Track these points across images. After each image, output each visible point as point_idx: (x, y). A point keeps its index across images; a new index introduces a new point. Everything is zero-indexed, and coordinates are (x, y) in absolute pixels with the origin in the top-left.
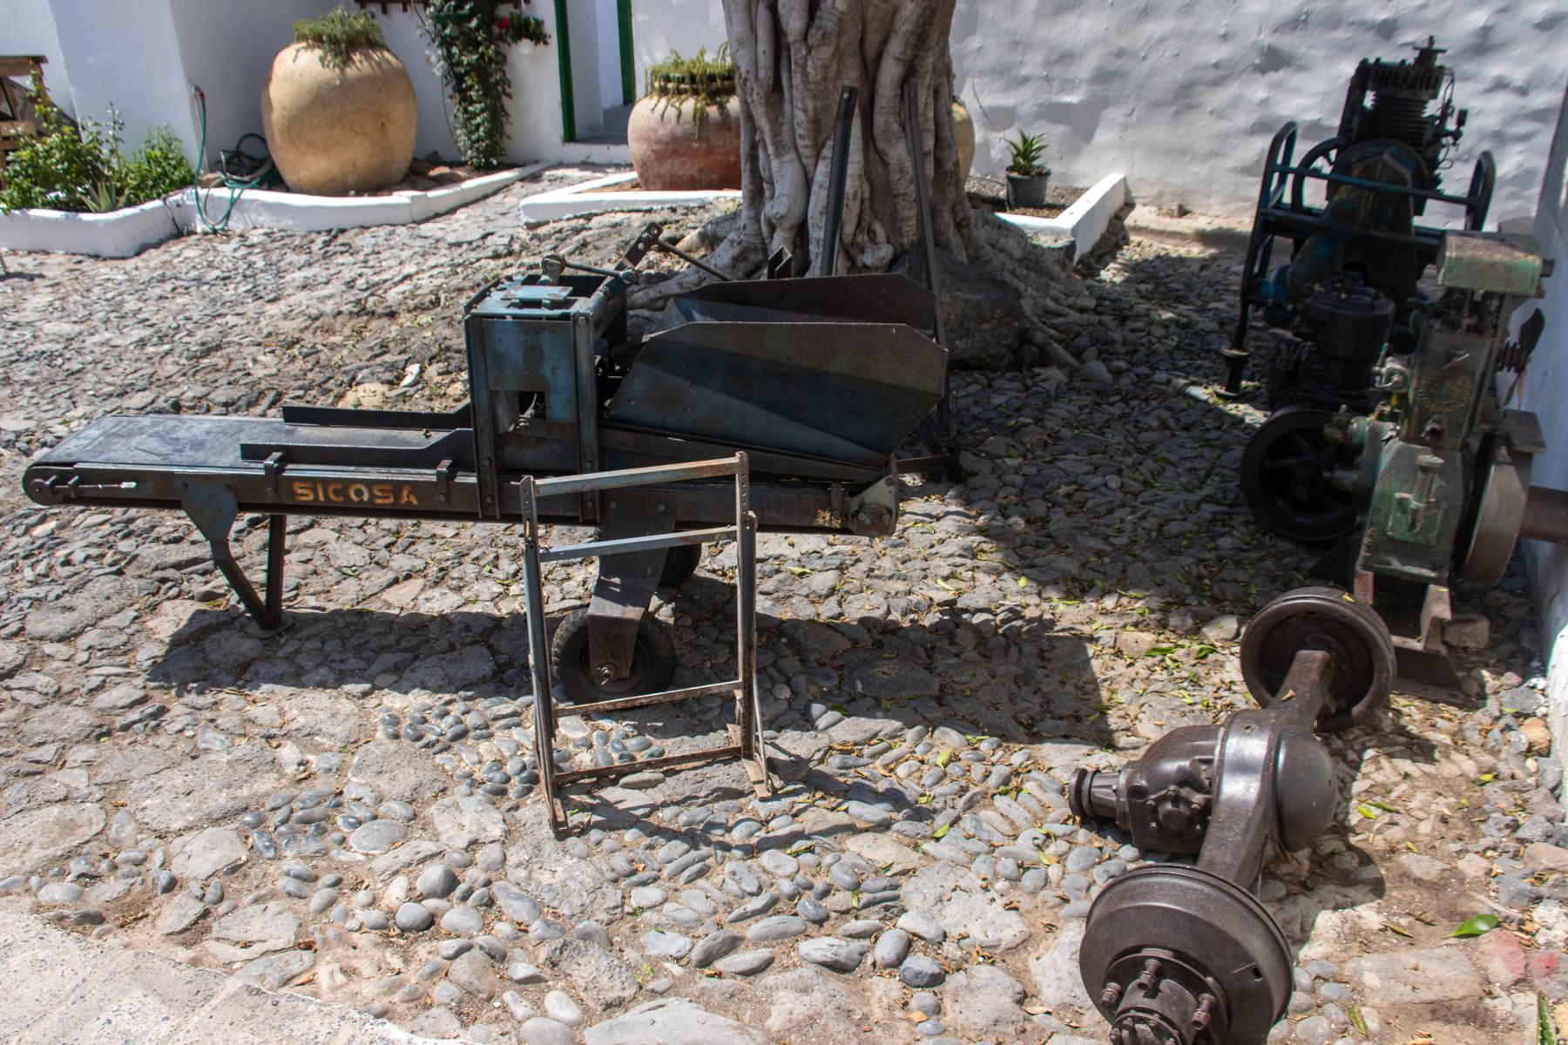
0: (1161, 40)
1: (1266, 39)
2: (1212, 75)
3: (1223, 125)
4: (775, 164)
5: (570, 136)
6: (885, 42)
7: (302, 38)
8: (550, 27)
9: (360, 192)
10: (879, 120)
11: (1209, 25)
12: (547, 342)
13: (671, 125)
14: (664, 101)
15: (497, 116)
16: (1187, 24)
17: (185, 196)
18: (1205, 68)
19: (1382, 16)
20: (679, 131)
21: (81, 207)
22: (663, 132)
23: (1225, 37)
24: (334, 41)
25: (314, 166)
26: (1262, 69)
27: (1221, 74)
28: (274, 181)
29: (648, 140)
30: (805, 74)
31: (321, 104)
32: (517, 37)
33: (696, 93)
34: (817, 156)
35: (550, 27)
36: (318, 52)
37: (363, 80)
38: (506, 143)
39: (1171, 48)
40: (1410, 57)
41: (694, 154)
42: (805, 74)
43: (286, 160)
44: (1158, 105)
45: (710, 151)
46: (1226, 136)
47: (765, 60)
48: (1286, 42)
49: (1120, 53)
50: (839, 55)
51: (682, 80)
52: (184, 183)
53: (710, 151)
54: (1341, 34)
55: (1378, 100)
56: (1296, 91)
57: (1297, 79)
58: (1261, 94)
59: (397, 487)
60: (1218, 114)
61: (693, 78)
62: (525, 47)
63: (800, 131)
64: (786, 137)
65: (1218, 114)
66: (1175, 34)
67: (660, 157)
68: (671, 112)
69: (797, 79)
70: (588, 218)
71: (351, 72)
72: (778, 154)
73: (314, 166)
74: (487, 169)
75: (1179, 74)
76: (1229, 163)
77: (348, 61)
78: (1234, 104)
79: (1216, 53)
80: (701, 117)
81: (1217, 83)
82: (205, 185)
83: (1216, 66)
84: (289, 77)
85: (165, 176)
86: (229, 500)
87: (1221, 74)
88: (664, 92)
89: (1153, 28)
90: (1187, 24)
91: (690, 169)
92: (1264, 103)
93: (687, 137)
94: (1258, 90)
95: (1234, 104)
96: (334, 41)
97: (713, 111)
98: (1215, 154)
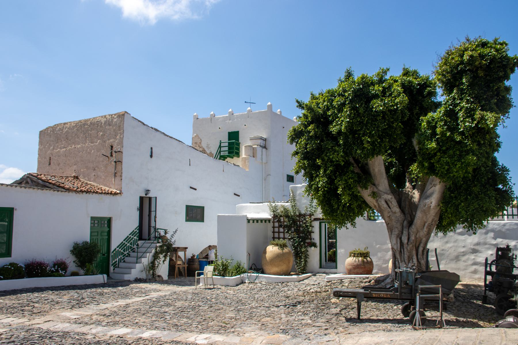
0: (451, 247)
1: (472, 247)
2: (463, 254)
4: (400, 264)
5: (321, 267)
6: (419, 244)
7: (273, 244)
8: (318, 244)
9: (285, 275)
10: (419, 257)
11: (460, 245)
12: (409, 275)
13: (357, 262)
14: (355, 258)
15: (306, 261)
17: (244, 275)
18: (461, 252)
19: (495, 243)
20: (359, 264)
21: (224, 276)
22: (355, 264)
23: (464, 247)
24: (281, 245)
25: (275, 269)
26: (473, 253)
27: (464, 254)
28: (263, 273)
31: (278, 257)
32: (311, 247)
33: (361, 256)
34: (409, 262)
35: (318, 244)
36: (277, 247)
37: (286, 253)
38: (307, 268)
39: (453, 249)
40: (505, 247)
41: (362, 268)
43: (266, 268)
44: (452, 260)
45: (365, 268)
46: (467, 266)
47: (399, 247)
48: (476, 247)
49: (443, 250)
50: (413, 246)
51: (358, 254)
52: (244, 272)
53: (365, 268)
54: (487, 246)
55: (502, 253)
56: (480, 257)
57: (480, 254)
59: (387, 294)
60: (465, 261)
61: (361, 254)
62: (313, 248)
63: (406, 258)
64: (403, 259)
65: (465, 261)
66: (453, 246)
67: (354, 268)
68: (357, 260)
69: (405, 250)
70: (341, 280)
71: (284, 251)
72: (401, 262)
73: (275, 269)
74: (303, 273)
75: (455, 254)
76: (468, 271)
77: (283, 249)
78: (468, 259)
79: (463, 250)
80: (363, 261)
81: (464, 255)
82: (248, 273)
83: (463, 252)
84: (271, 252)
85: (239, 270)
86: (363, 296)
87: (464, 254)
88: (354, 256)
90: (456, 244)
91: (361, 271)
92: (474, 259)
93: (360, 265)
94: (472, 257)
95: (468, 259)
96: (281, 245)
97: (365, 260)
98: (465, 269)
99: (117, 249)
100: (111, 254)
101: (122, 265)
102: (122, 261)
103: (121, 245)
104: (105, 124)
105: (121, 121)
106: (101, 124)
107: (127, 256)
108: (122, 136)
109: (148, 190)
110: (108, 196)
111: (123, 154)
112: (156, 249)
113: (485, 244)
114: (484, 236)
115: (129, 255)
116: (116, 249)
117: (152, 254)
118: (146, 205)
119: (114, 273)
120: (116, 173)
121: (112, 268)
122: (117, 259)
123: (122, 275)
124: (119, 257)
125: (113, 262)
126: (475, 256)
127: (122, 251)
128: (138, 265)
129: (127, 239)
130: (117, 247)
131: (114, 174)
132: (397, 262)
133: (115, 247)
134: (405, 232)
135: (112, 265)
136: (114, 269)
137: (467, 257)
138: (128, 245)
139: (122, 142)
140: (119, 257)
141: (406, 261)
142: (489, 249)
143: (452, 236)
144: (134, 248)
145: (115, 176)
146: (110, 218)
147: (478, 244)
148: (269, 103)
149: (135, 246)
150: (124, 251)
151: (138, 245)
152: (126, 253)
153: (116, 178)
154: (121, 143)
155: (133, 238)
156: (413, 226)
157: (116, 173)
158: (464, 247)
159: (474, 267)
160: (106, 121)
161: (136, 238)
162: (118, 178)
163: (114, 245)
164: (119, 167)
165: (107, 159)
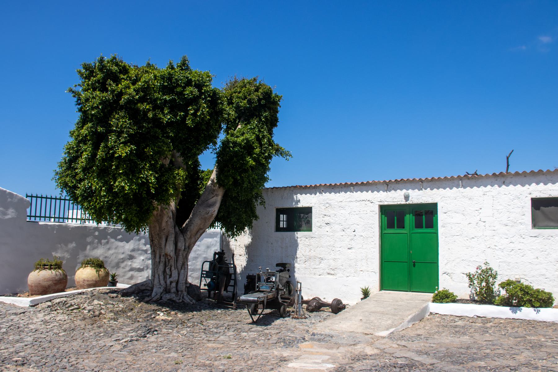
1: (129, 253)
2: (122, 260)
3: (124, 270)
11: (120, 251)
16: (116, 251)
20: (61, 277)
22: (57, 278)
23: (123, 253)
27: (123, 260)
29: (52, 281)
30: (183, 255)
42: (183, 255)
46: (125, 272)
48: (133, 253)
49: (106, 257)
54: (140, 252)
56: (135, 263)
57: (134, 260)
58: (130, 263)
60: (123, 268)
66: (115, 253)
67: (56, 284)
75: (116, 261)
76: (126, 277)
78: (126, 266)
79: (122, 256)
81: (123, 262)
87: (123, 260)
89: (111, 252)
90: (116, 251)
92: (131, 265)
94: (129, 263)
95: (126, 266)
98: (124, 276)
113: (138, 250)
114: (138, 242)
126: (132, 262)
132: (168, 271)
134: (181, 238)
137: (125, 263)
141: (180, 267)
142: (141, 254)
143: (113, 242)
147: (133, 250)
156: (188, 233)
158: (123, 253)
159: (131, 273)
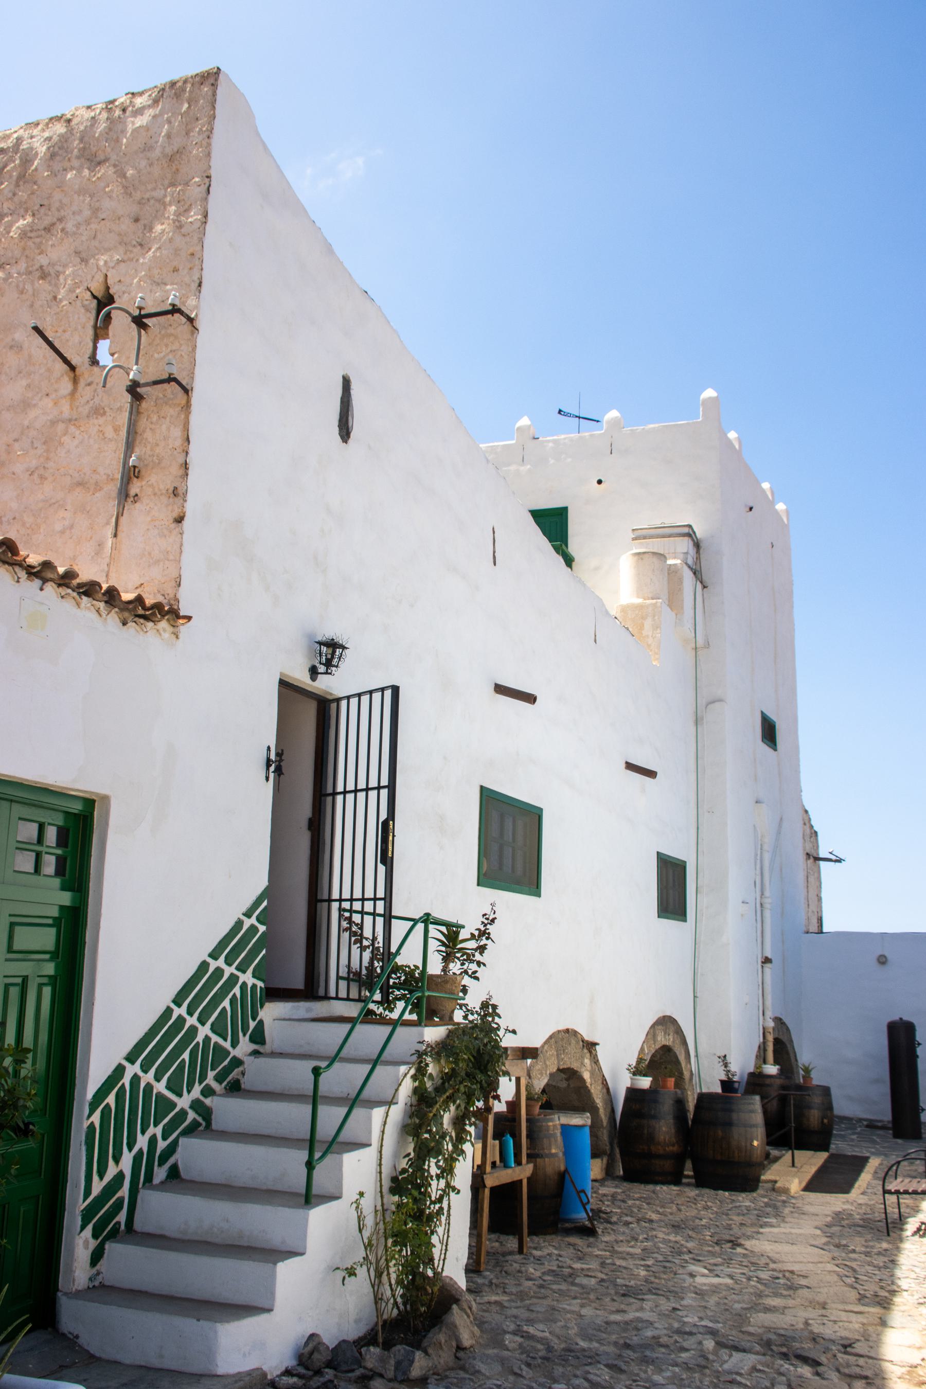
99: (132, 1069)
100: (83, 1120)
101: (161, 1208)
102: (160, 1174)
103: (161, 1039)
104: (52, 155)
105: (190, 120)
106: (27, 160)
107: (191, 1130)
108: (194, 216)
109: (333, 645)
110: (87, 613)
111: (202, 339)
112: (421, 1071)
115: (203, 1123)
116: (119, 1071)
117: (397, 1112)
118: (313, 742)
119: (100, 1290)
120: (131, 474)
121: (80, 1244)
122: (127, 1159)
123: (187, 1325)
124: (142, 1142)
125: (97, 1187)
127: (160, 1087)
128: (319, 1220)
129: (198, 988)
130: (131, 1058)
131: (113, 488)
133: (118, 1056)
135: (87, 1215)
136: (97, 1256)
138: (204, 1031)
139: (196, 258)
140: (142, 1142)
144: (237, 1062)
145: (124, 495)
146: (90, 803)
148: (709, 393)
149: (245, 1046)
150: (175, 1087)
151: (258, 1037)
152: (183, 1102)
153: (136, 514)
154: (189, 262)
155: (233, 979)
157: (131, 474)
160: (64, 139)
161: (247, 978)
162: (147, 514)
163: (111, 1036)
164: (159, 432)
165: (66, 386)
